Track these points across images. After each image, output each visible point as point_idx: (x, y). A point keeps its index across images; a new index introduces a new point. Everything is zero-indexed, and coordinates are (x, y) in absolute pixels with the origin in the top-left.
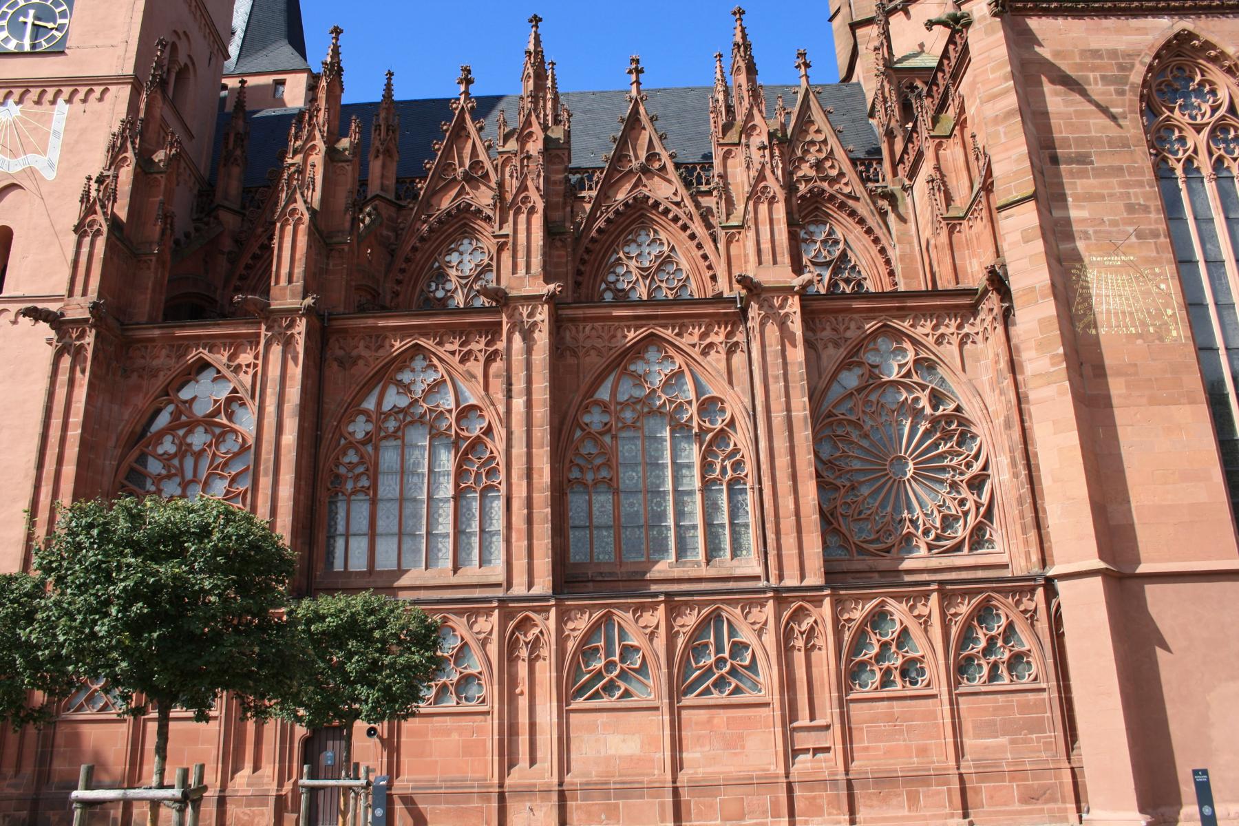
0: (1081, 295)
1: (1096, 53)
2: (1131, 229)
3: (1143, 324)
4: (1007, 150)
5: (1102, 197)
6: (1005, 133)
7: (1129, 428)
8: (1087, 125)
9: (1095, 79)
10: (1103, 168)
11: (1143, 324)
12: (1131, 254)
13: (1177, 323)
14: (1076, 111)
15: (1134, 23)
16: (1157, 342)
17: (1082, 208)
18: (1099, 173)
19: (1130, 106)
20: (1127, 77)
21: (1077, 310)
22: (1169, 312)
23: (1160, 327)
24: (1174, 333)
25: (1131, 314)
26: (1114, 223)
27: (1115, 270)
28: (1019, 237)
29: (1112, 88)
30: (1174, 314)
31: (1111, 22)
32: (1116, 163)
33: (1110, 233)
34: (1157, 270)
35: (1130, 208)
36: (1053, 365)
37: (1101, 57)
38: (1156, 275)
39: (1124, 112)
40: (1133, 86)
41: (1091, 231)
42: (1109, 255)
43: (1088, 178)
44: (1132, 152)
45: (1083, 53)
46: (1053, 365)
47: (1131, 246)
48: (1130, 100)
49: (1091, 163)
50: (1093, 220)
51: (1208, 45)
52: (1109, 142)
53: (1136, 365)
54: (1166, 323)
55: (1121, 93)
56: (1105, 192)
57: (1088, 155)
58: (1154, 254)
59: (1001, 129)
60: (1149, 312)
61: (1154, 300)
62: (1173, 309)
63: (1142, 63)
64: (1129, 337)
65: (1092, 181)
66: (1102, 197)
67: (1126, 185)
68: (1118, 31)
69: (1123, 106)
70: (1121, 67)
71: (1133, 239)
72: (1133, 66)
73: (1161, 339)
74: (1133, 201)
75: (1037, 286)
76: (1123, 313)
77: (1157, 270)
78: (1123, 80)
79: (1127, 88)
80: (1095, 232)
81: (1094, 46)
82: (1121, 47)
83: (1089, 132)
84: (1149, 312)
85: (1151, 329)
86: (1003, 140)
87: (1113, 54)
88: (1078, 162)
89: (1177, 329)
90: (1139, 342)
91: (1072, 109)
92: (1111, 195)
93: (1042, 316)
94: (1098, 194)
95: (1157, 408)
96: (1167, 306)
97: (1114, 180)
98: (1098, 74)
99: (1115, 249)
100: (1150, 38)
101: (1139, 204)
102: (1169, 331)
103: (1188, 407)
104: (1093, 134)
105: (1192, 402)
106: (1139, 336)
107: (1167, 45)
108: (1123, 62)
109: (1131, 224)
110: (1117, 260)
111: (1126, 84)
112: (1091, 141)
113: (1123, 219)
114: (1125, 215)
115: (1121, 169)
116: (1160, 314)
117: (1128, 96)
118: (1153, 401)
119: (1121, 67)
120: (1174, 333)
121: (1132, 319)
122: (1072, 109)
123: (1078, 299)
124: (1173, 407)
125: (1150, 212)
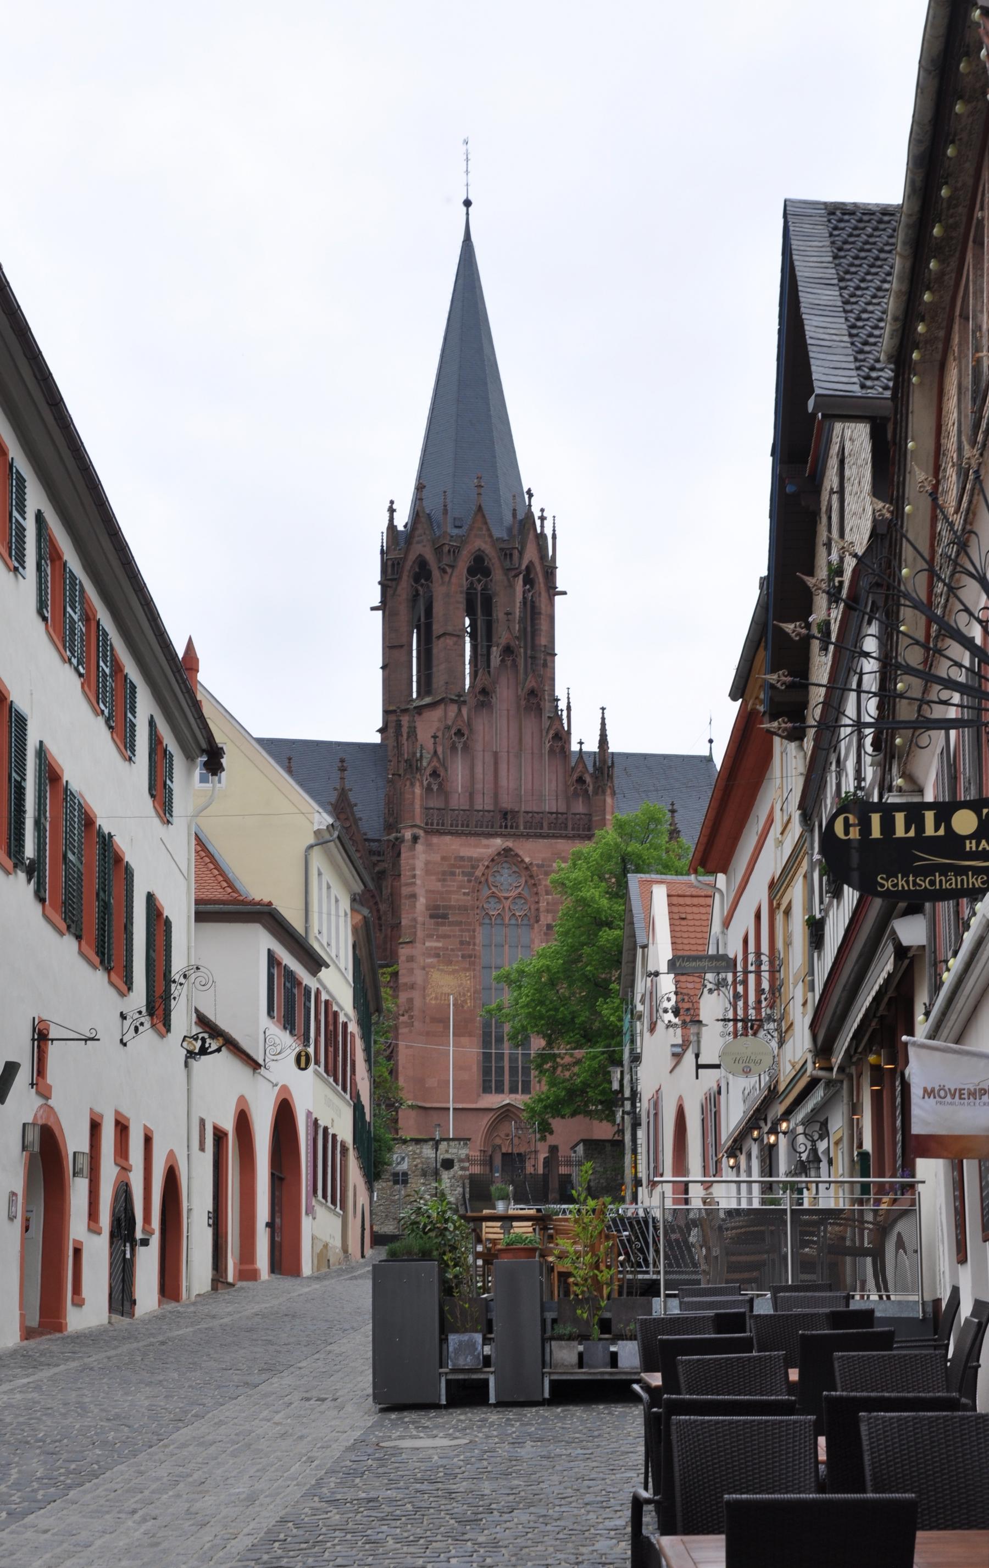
1: (462, 858)
5: (449, 937)
15: (485, 841)
18: (452, 924)
26: (452, 950)
27: (449, 973)
31: (472, 840)
35: (462, 943)
37: (464, 861)
45: (456, 858)
51: (517, 855)
57: (448, 914)
66: (449, 937)
67: (462, 931)
68: (476, 846)
73: (463, 1007)
81: (462, 854)
82: (475, 855)
87: (470, 859)
92: (454, 936)
96: (468, 991)
99: (450, 963)
100: (490, 850)
107: (499, 854)
108: (474, 863)
110: (450, 968)
112: (450, 907)
116: (464, 995)
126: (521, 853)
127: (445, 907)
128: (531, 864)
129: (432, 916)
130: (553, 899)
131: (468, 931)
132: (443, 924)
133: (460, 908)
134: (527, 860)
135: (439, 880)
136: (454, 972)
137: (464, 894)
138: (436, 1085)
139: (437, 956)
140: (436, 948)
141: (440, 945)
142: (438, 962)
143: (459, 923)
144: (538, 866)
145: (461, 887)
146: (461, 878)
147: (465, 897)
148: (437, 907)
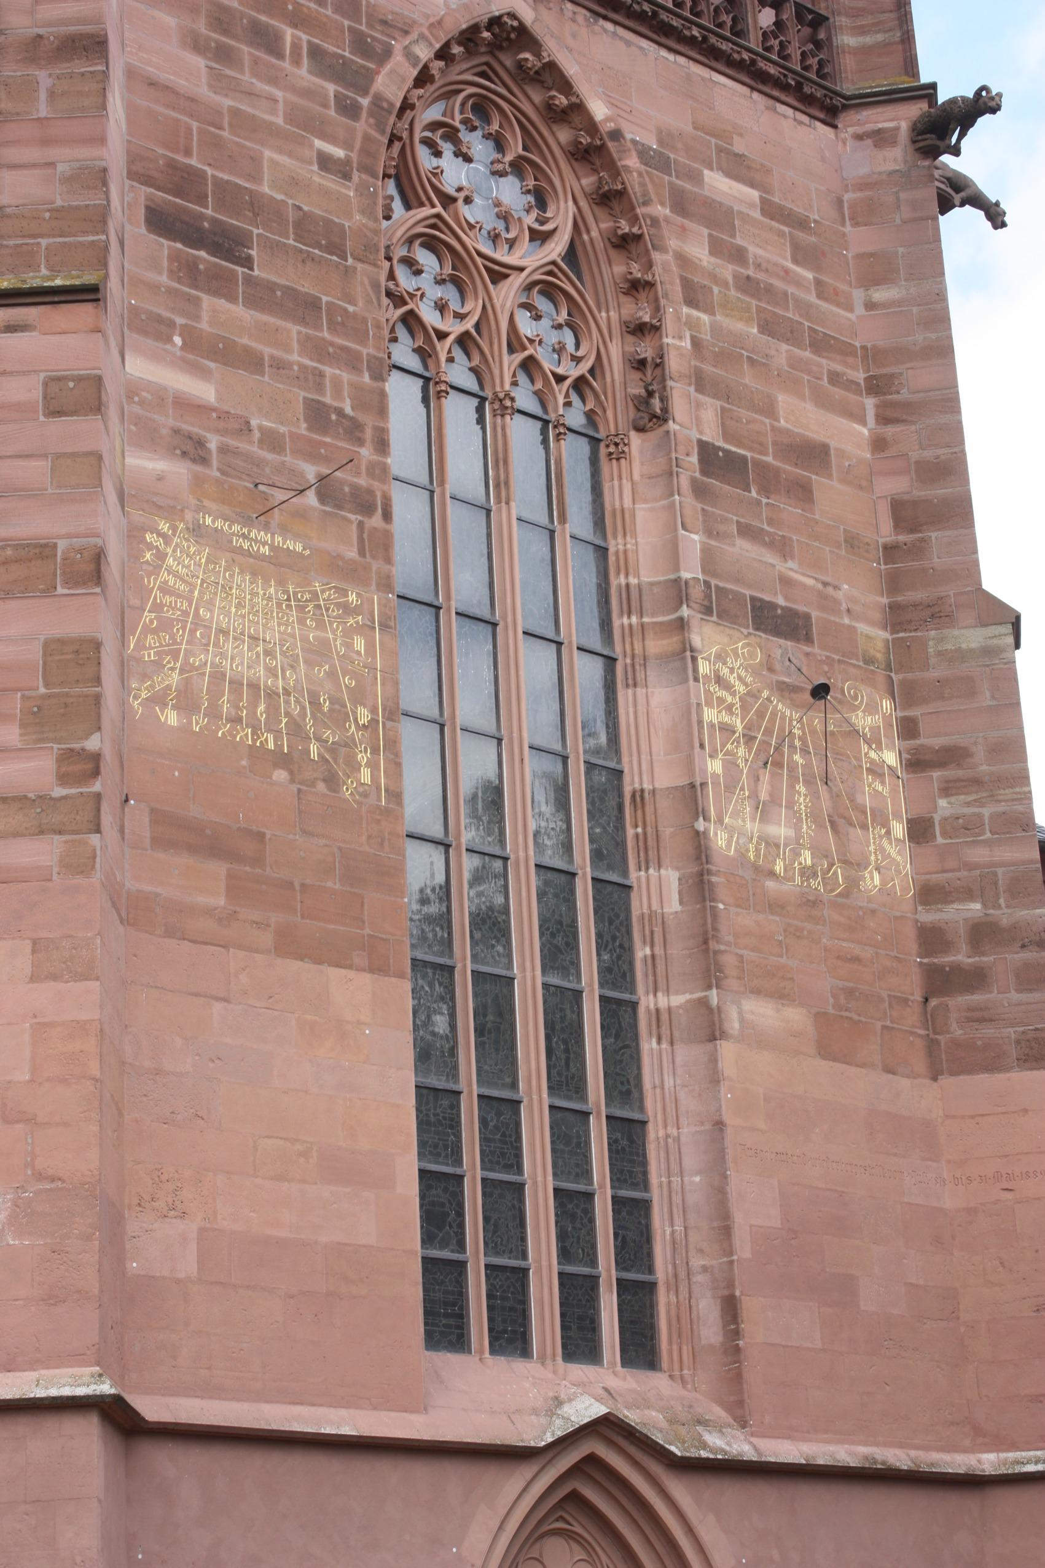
0: (157, 608)
2: (311, 471)
3: (296, 729)
4: (46, 142)
5: (253, 362)
6: (52, 95)
7: (218, 1007)
8: (255, 160)
9: (296, 47)
10: (271, 287)
11: (296, 729)
12: (296, 537)
13: (375, 751)
14: (235, 112)
16: (321, 787)
17: (203, 374)
18: (262, 296)
19: (365, 152)
20: (369, 77)
21: (140, 646)
22: (364, 715)
23: (333, 749)
24: (365, 775)
25: (272, 695)
26: (272, 441)
27: (259, 567)
28: (37, 395)
29: (331, 88)
30: (374, 722)
32: (305, 287)
33: (259, 463)
34: (352, 598)
35: (318, 415)
36: (63, 779)
38: (348, 610)
39: (348, 161)
40: (378, 99)
41: (213, 443)
42: (248, 522)
43: (232, 298)
44: (348, 272)
46: (63, 779)
47: (301, 515)
48: (367, 138)
49: (248, 262)
50: (223, 415)
52: (299, 225)
53: (261, 836)
54: (349, 744)
55: (350, 110)
56: (267, 351)
58: (352, 553)
59: (44, 78)
60: (315, 704)
61: (332, 674)
62: (374, 710)
63: (409, 54)
64: (257, 753)
65: (239, 310)
66: (253, 362)
69: (348, 145)
70: (361, 45)
71: (311, 499)
72: (387, 53)
73: (332, 781)
74: (328, 399)
75: (62, 545)
76: (254, 686)
77: (352, 598)
78: (361, 81)
79: (365, 102)
80: (223, 450)
83: (256, 178)
84: (315, 704)
85: (314, 749)
86: (43, 111)
88: (216, 249)
89: (373, 765)
90: (280, 775)
91: (227, 102)
92: (279, 365)
93: (57, 632)
94: (247, 350)
95: (295, 965)
96: (359, 696)
97: (294, 329)
98: (305, 37)
99: (262, 514)
101: (340, 412)
102: (354, 767)
103: (367, 978)
104: (266, 189)
105: (378, 968)
106: (282, 760)
109: (313, 457)
110: (262, 541)
111: (365, 92)
112: (256, 206)
113: (295, 437)
114: (303, 428)
115: (314, 304)
116: (339, 716)
117: (362, 126)
118: (288, 945)
119: (361, 45)
120: (365, 775)
121: (273, 710)
122: (227, 102)
123: (147, 616)
124: (334, 973)
125: (361, 442)
126: (571, 68)
127: (227, 195)
128: (616, 135)
129: (159, 221)
130: (715, 329)
131: (352, 361)
132: (221, 285)
133: (304, 225)
134: (599, 110)
135: (197, 45)
136: (280, 565)
137: (325, 162)
138: (188, 1266)
139: (192, 450)
140: (184, 404)
141: (205, 391)
142: (198, 482)
143: (306, 308)
144: (644, 153)
145: (307, 123)
146: (304, 74)
147: (330, 182)
148: (185, 182)
